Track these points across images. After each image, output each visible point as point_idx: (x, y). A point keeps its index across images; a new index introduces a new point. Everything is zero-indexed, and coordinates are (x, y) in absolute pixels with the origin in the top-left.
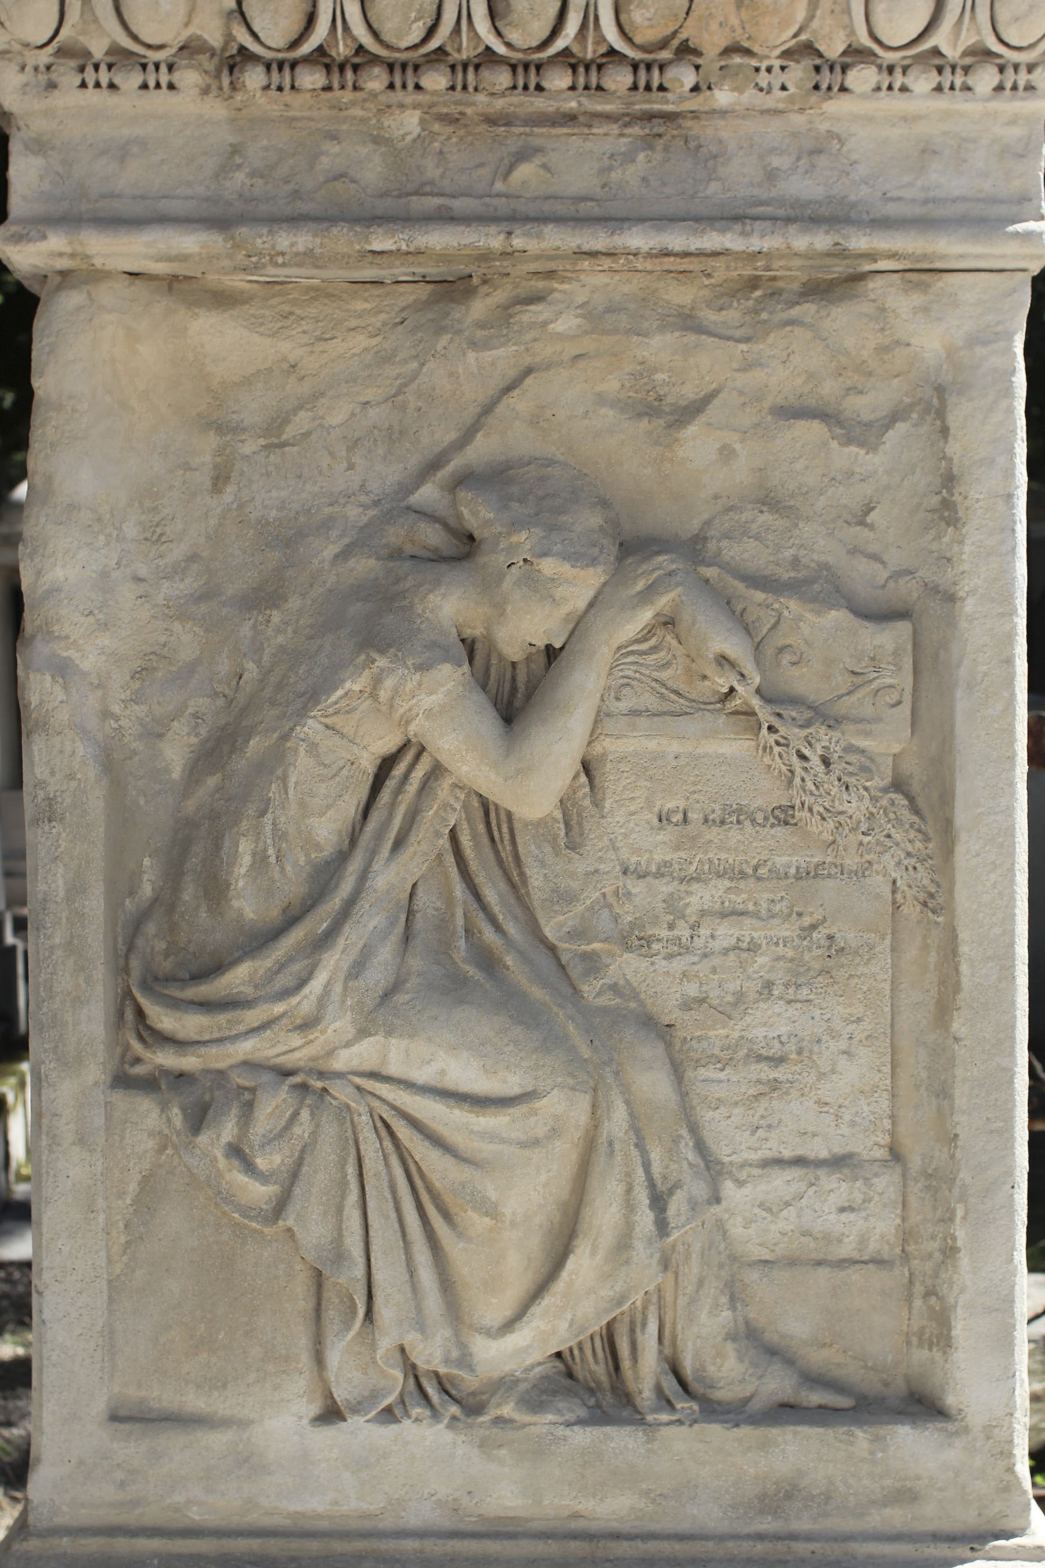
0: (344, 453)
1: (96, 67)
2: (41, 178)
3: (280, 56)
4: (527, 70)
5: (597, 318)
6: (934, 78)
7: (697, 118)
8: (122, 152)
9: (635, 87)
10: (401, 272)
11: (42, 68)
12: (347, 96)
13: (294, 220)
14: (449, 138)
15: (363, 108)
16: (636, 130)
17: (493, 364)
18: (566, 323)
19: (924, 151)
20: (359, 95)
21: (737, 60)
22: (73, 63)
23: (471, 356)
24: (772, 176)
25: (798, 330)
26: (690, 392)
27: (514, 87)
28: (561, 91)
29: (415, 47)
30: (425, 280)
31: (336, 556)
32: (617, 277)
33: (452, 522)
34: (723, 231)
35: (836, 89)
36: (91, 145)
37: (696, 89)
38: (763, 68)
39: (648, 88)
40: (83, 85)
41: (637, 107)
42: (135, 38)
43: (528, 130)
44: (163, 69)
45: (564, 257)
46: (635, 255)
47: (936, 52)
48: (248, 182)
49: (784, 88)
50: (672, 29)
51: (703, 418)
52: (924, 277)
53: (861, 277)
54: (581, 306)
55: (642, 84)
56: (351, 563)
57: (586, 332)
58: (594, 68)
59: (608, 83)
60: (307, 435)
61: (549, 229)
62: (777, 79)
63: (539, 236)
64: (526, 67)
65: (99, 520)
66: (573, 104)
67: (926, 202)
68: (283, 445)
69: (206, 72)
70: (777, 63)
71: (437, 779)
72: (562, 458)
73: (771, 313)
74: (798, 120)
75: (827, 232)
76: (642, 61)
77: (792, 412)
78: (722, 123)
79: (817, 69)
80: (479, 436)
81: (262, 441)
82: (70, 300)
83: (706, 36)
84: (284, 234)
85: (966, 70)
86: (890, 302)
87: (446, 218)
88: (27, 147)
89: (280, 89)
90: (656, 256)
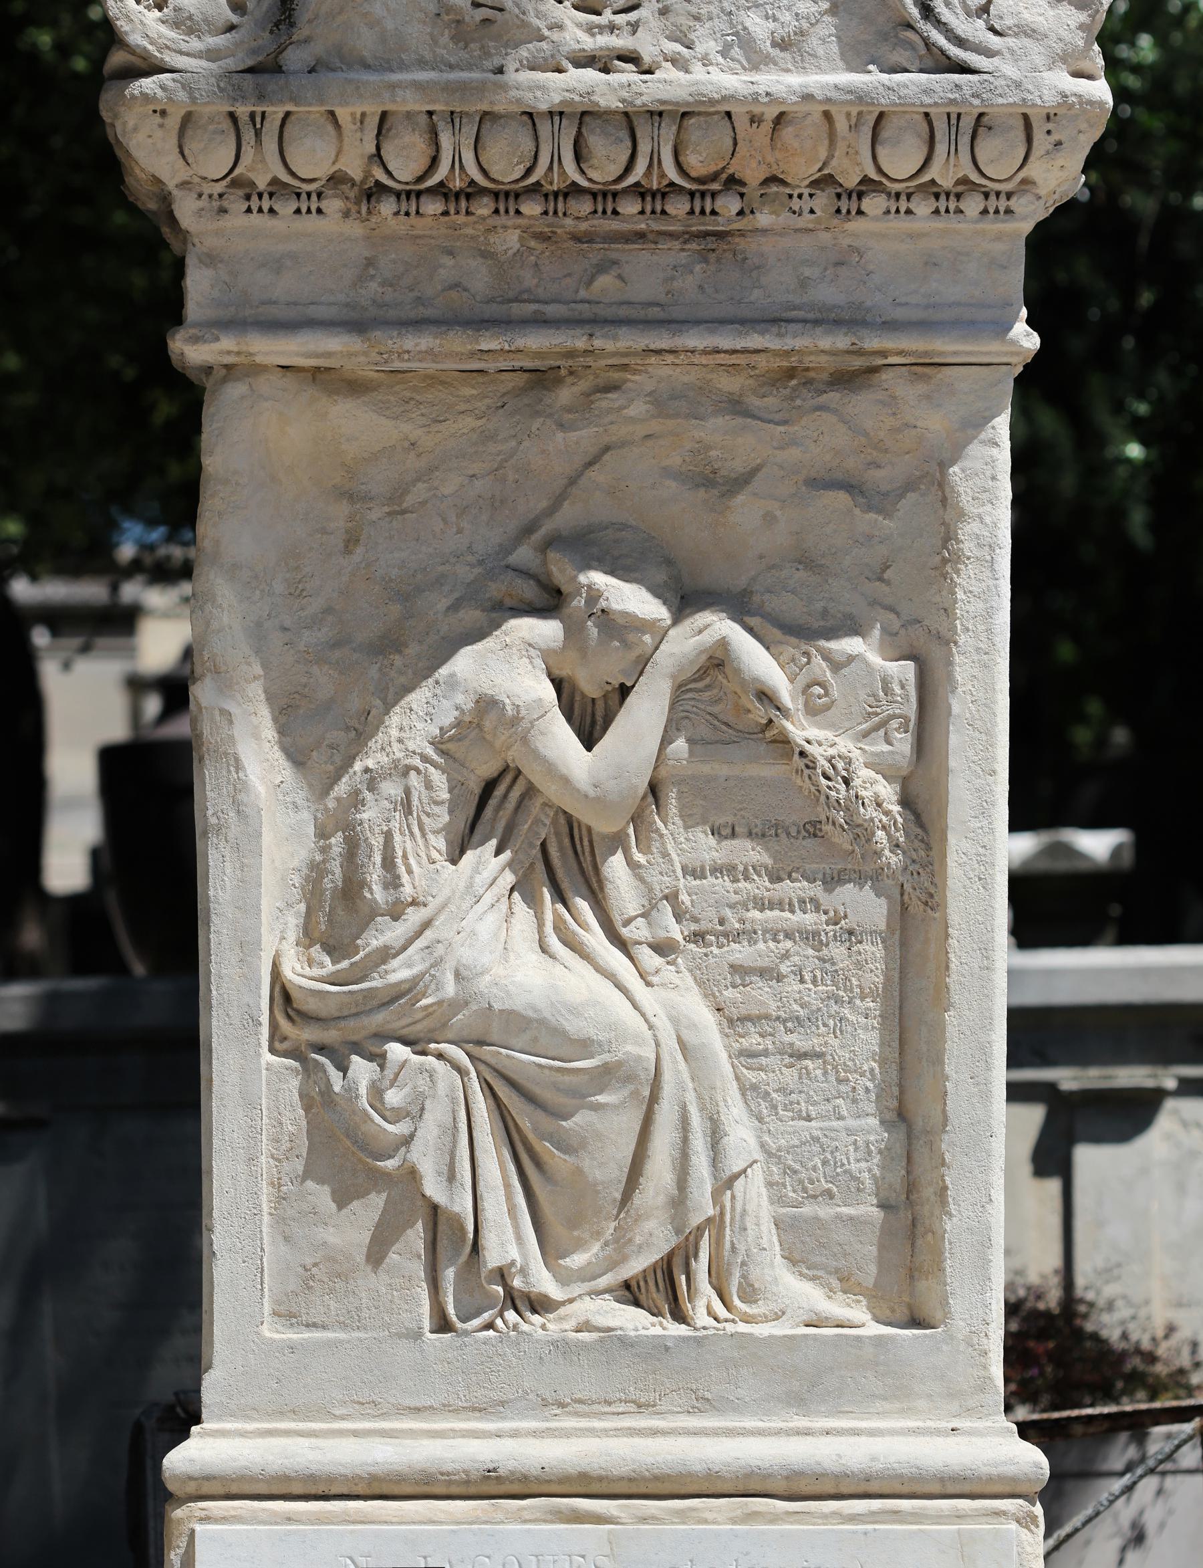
0: (454, 519)
1: (260, 196)
2: (212, 286)
3: (408, 187)
4: (605, 196)
5: (661, 404)
6: (932, 204)
7: (743, 235)
8: (276, 265)
9: (692, 212)
10: (503, 365)
11: (216, 196)
12: (461, 219)
13: (417, 324)
14: (543, 252)
15: (474, 229)
16: (694, 246)
17: (577, 443)
18: (638, 408)
19: (926, 263)
20: (470, 218)
21: (774, 189)
22: (241, 192)
23: (560, 435)
24: (803, 283)
25: (824, 415)
26: (738, 465)
27: (595, 212)
28: (633, 216)
29: (517, 181)
30: (522, 370)
31: (448, 608)
32: (678, 370)
33: (543, 578)
34: (762, 333)
35: (854, 213)
36: (252, 259)
37: (741, 213)
38: (795, 195)
39: (703, 212)
40: (249, 210)
41: (694, 229)
42: (293, 174)
43: (606, 246)
44: (314, 197)
45: (635, 354)
46: (692, 352)
47: (933, 182)
48: (380, 290)
49: (812, 211)
50: (721, 166)
51: (749, 489)
52: (927, 370)
53: (874, 370)
54: (650, 394)
55: (697, 210)
56: (461, 614)
57: (653, 416)
58: (659, 197)
59: (669, 209)
60: (423, 503)
61: (623, 331)
62: (806, 204)
63: (615, 338)
64: (605, 195)
65: (256, 577)
66: (643, 226)
67: (927, 307)
68: (403, 512)
69: (347, 198)
70: (806, 192)
71: (530, 799)
72: (634, 523)
73: (804, 400)
74: (825, 237)
75: (846, 334)
76: (698, 190)
77: (820, 483)
78: (763, 240)
79: (839, 196)
80: (566, 504)
81: (386, 509)
82: (235, 391)
83: (748, 172)
84: (410, 337)
85: (958, 196)
86: (899, 392)
87: (541, 322)
88: (201, 261)
89: (407, 214)
90: (710, 353)
